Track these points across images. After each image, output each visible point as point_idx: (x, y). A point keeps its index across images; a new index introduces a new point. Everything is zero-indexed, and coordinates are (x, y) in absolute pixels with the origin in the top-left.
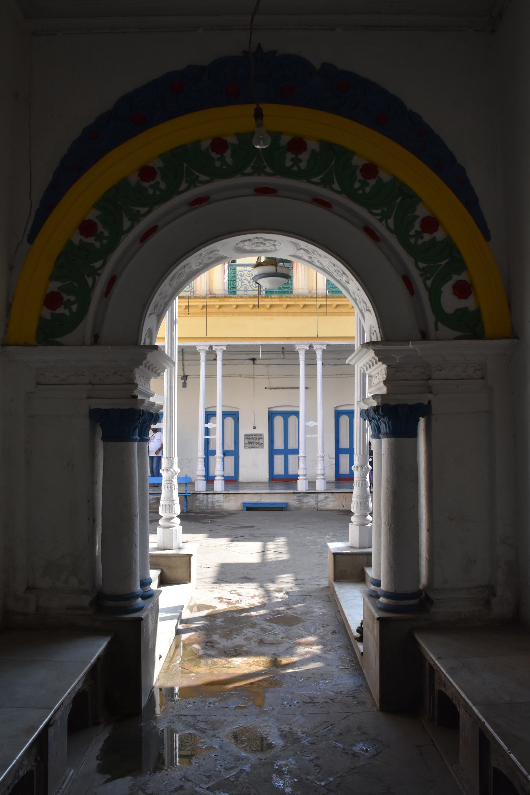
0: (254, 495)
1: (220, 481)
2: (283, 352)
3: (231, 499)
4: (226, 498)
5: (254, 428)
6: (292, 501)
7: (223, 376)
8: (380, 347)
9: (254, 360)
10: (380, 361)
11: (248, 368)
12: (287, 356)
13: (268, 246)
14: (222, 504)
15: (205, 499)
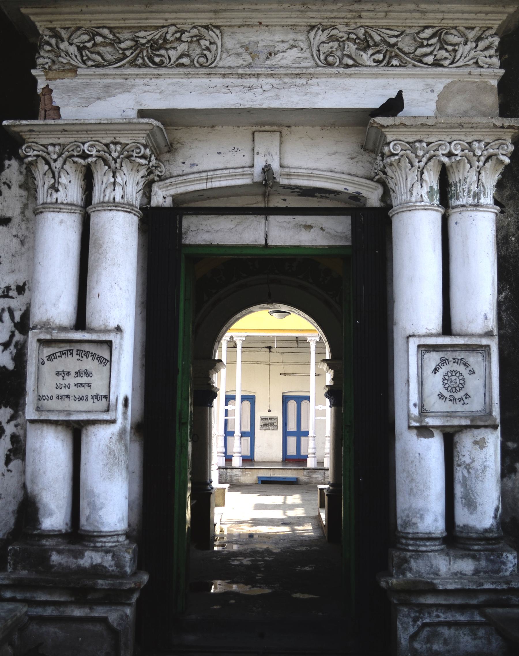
0: (268, 470)
1: (238, 458)
2: (297, 341)
3: (247, 474)
4: (243, 472)
5: (269, 411)
6: (302, 476)
7: (242, 362)
8: (329, 362)
9: (270, 348)
10: (330, 368)
11: (264, 355)
12: (301, 345)
13: (276, 306)
14: (240, 478)
15: (225, 473)
